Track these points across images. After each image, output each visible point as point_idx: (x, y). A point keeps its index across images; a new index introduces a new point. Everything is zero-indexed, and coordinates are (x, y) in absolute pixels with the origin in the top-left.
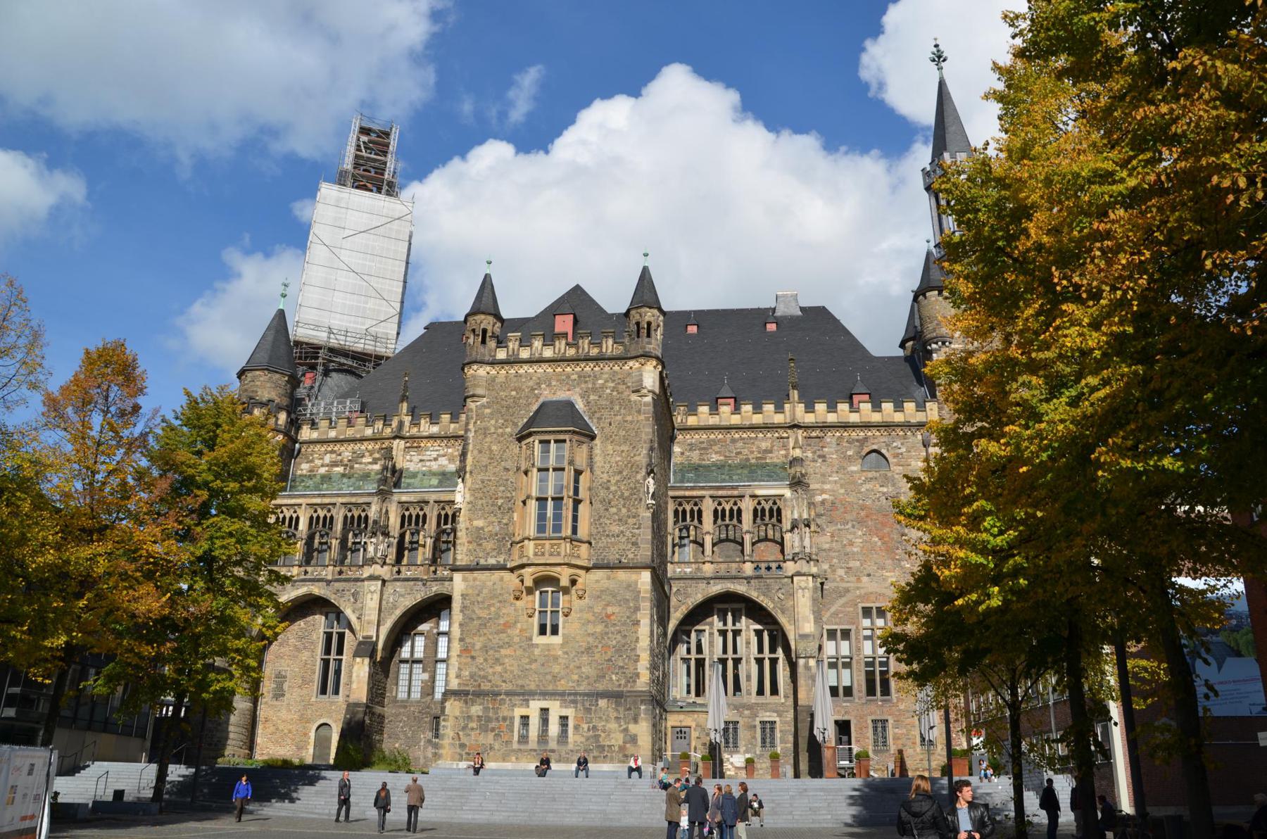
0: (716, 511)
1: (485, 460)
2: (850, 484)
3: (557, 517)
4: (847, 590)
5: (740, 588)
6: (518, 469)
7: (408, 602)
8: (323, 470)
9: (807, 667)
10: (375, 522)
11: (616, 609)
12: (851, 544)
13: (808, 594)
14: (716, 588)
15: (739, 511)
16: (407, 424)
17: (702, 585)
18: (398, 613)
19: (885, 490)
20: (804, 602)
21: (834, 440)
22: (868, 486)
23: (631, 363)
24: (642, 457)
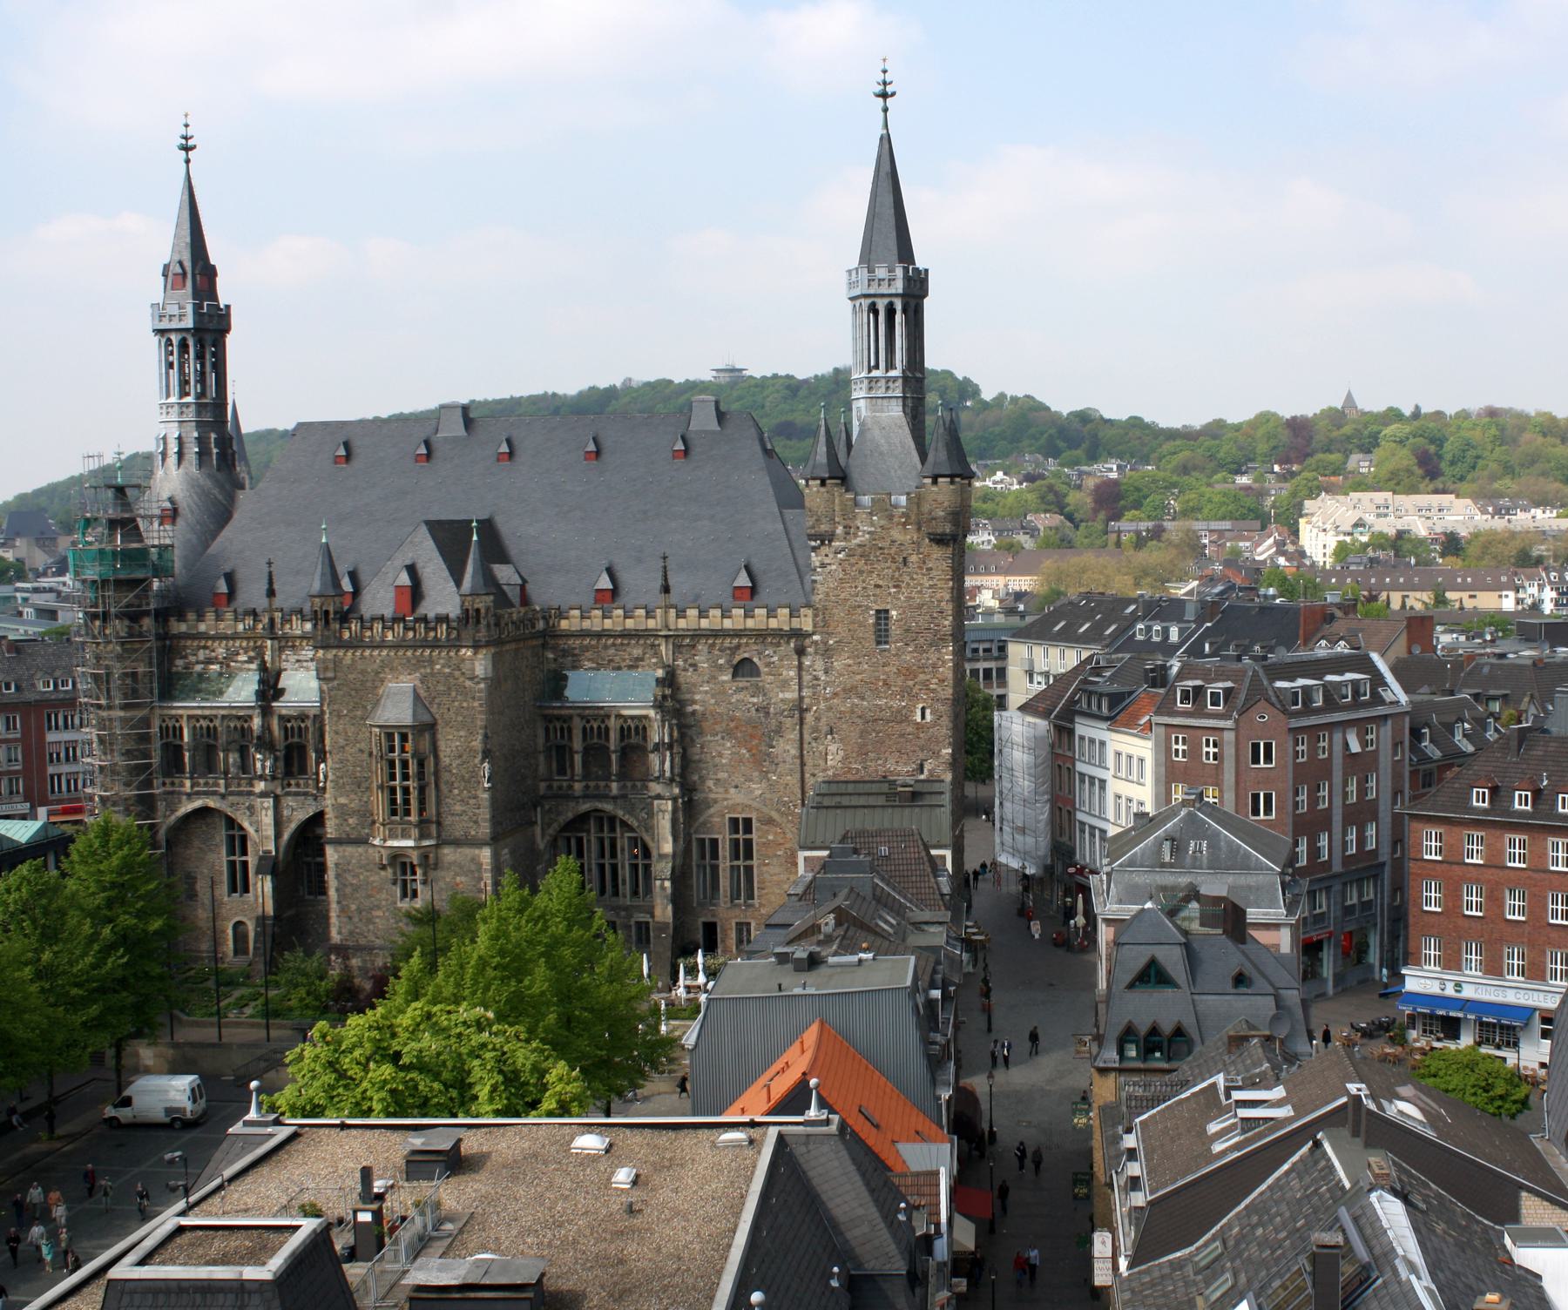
0: (584, 729)
1: (342, 742)
2: (720, 694)
3: (406, 802)
4: (716, 801)
5: (608, 807)
6: (371, 754)
7: (301, 815)
8: (199, 668)
9: (663, 888)
10: (259, 738)
11: (463, 879)
12: (720, 755)
13: (668, 816)
14: (585, 807)
15: (607, 729)
16: (278, 621)
17: (572, 804)
18: (293, 826)
19: (755, 700)
20: (664, 824)
21: (706, 649)
22: (740, 696)
23: (463, 651)
24: (477, 743)
